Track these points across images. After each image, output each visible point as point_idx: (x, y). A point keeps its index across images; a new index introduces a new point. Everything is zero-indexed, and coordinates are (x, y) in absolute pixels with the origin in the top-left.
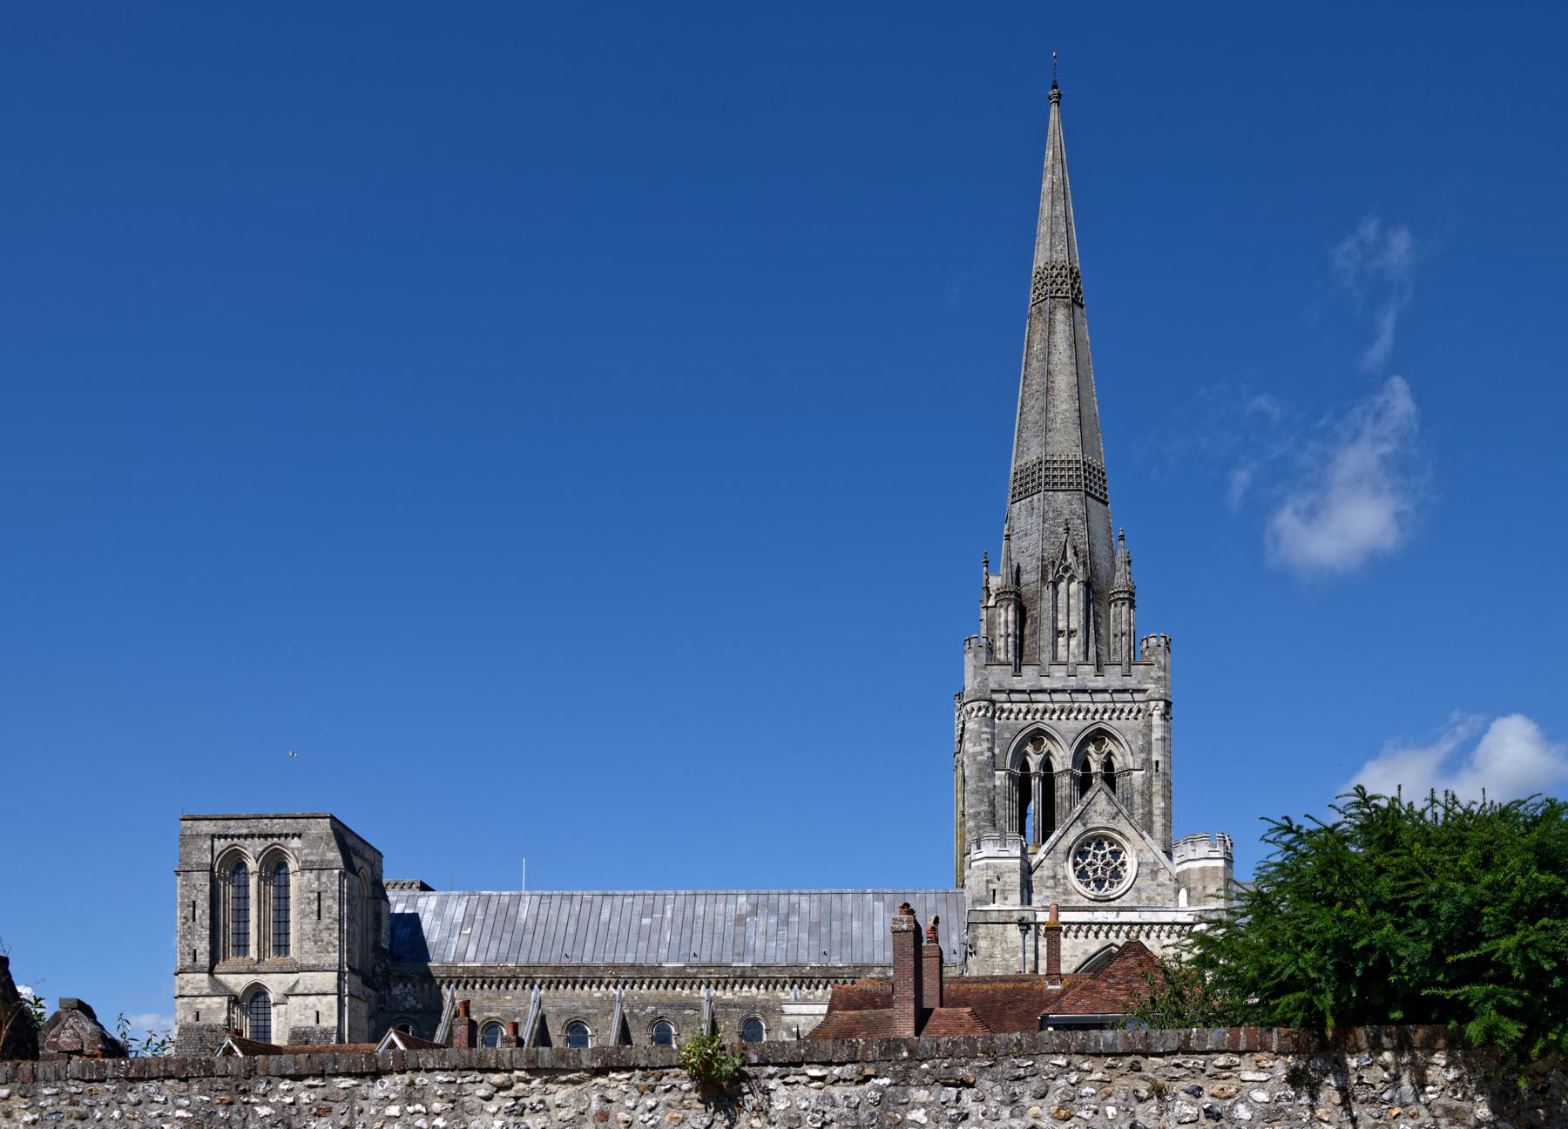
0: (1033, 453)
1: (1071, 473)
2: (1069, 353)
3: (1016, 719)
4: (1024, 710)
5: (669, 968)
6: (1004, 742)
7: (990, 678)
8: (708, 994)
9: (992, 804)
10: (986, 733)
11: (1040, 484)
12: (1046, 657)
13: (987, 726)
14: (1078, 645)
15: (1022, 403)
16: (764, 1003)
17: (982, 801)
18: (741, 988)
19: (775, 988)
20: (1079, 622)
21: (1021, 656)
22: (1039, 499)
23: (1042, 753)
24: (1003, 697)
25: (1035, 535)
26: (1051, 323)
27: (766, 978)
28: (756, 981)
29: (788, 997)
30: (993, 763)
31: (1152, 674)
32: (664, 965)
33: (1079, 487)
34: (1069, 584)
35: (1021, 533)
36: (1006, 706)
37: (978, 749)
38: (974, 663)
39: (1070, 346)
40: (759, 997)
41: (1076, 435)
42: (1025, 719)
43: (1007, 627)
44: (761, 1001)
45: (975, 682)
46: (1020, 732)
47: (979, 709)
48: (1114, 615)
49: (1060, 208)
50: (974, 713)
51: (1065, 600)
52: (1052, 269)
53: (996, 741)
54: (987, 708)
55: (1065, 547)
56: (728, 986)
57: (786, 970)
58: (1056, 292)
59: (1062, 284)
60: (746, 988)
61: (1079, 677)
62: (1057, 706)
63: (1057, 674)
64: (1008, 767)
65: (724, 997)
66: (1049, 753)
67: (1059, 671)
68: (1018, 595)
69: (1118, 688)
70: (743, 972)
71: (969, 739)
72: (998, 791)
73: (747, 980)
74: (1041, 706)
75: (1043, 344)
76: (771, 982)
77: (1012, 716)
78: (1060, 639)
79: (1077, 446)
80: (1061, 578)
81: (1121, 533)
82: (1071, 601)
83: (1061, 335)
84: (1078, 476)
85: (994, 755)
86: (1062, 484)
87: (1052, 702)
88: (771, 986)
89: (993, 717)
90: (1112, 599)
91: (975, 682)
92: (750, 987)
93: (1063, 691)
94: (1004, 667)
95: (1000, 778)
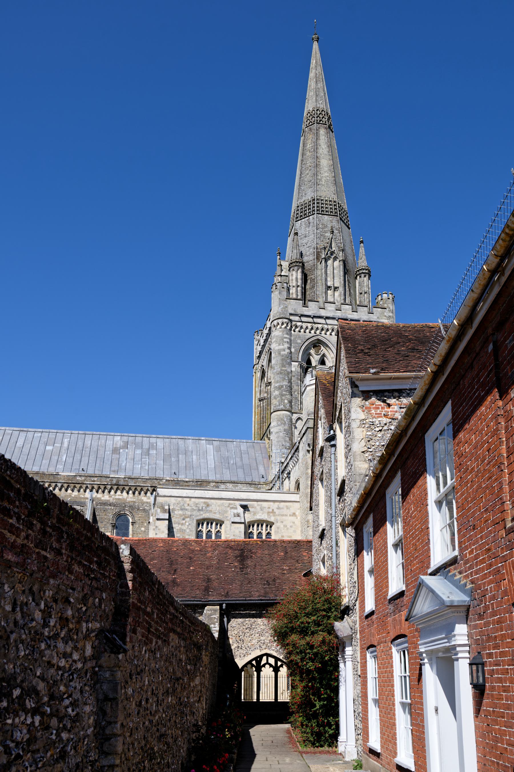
0: (309, 195)
1: (331, 207)
2: (327, 150)
3: (305, 332)
4: (310, 327)
5: (64, 476)
6: (297, 345)
7: (289, 307)
8: (91, 496)
9: (290, 381)
10: (286, 338)
11: (314, 211)
12: (321, 300)
13: (287, 334)
14: (340, 295)
15: (301, 173)
16: (132, 504)
17: (284, 379)
18: (116, 492)
19: (140, 494)
20: (340, 282)
21: (304, 299)
22: (313, 218)
23: (320, 354)
24: (297, 318)
25: (313, 236)
26: (317, 135)
27: (134, 486)
28: (127, 488)
29: (149, 501)
30: (290, 358)
31: (385, 314)
32: (60, 474)
33: (336, 214)
34: (334, 262)
35: (302, 236)
36: (299, 324)
37: (281, 347)
38: (279, 297)
39: (328, 146)
40: (128, 500)
41: (333, 188)
42: (310, 333)
43: (297, 281)
44: (129, 502)
45: (280, 308)
46: (307, 340)
47: (283, 324)
48: (359, 283)
49: (320, 85)
50: (279, 327)
51: (332, 270)
52: (317, 110)
53: (293, 344)
54: (287, 324)
55: (331, 241)
56: (106, 491)
57: (149, 481)
58: (320, 121)
59: (322, 118)
60: (119, 492)
61: (343, 311)
62: (330, 327)
63: (329, 308)
64: (300, 360)
65: (102, 498)
66: (324, 355)
67: (331, 307)
68: (303, 265)
69: (366, 320)
70: (118, 481)
71: (276, 341)
72: (293, 374)
73: (120, 487)
74: (320, 326)
75: (313, 144)
76: (137, 490)
77: (302, 330)
78: (329, 292)
79: (334, 194)
80: (329, 258)
81: (361, 240)
82: (335, 271)
83: (323, 141)
84: (335, 209)
85: (291, 352)
86: (327, 211)
87: (327, 324)
88: (137, 492)
89: (291, 330)
90: (358, 273)
91: (280, 308)
92: (122, 492)
93: (333, 318)
94: (297, 301)
95: (294, 366)
